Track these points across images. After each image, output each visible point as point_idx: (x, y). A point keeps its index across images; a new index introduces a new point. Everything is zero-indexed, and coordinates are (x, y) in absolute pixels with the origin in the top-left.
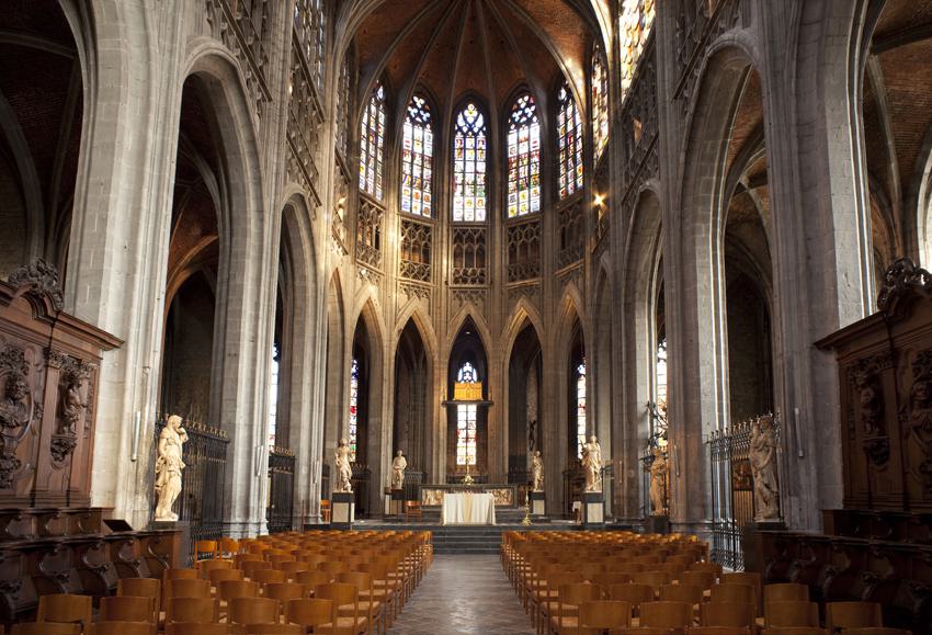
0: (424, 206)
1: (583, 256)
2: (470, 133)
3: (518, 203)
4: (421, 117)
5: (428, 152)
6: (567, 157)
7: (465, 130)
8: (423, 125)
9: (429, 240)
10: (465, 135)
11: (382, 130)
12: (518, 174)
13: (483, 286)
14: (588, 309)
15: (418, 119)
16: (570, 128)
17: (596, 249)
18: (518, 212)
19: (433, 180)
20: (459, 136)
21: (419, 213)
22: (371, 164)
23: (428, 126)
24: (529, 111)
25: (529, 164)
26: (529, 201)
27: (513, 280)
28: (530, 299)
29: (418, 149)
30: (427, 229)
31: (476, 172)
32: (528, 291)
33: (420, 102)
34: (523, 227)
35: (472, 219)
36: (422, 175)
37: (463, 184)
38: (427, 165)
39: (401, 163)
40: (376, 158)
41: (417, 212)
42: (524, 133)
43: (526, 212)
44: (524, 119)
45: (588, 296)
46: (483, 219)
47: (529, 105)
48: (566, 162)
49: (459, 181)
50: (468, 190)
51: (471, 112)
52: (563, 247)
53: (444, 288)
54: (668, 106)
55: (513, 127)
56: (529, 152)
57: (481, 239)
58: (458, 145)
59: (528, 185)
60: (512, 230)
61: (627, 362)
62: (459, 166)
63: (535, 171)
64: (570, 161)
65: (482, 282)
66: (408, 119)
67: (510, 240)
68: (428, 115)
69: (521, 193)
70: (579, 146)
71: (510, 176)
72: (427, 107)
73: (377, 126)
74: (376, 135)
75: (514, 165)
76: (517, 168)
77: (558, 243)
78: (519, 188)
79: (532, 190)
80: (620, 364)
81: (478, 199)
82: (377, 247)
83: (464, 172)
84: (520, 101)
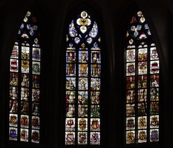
2: (83, 45)
7: (77, 41)
10: (77, 47)
12: (136, 97)
19: (42, 100)
20: (70, 48)
25: (149, 87)
29: (25, 70)
31: (90, 89)
37: (76, 103)
39: (8, 88)
49: (71, 99)
58: (69, 59)
63: (155, 98)
68: (36, 27)
71: (128, 98)
75: (132, 85)
76: (136, 90)
78: (137, 113)
83: (76, 90)
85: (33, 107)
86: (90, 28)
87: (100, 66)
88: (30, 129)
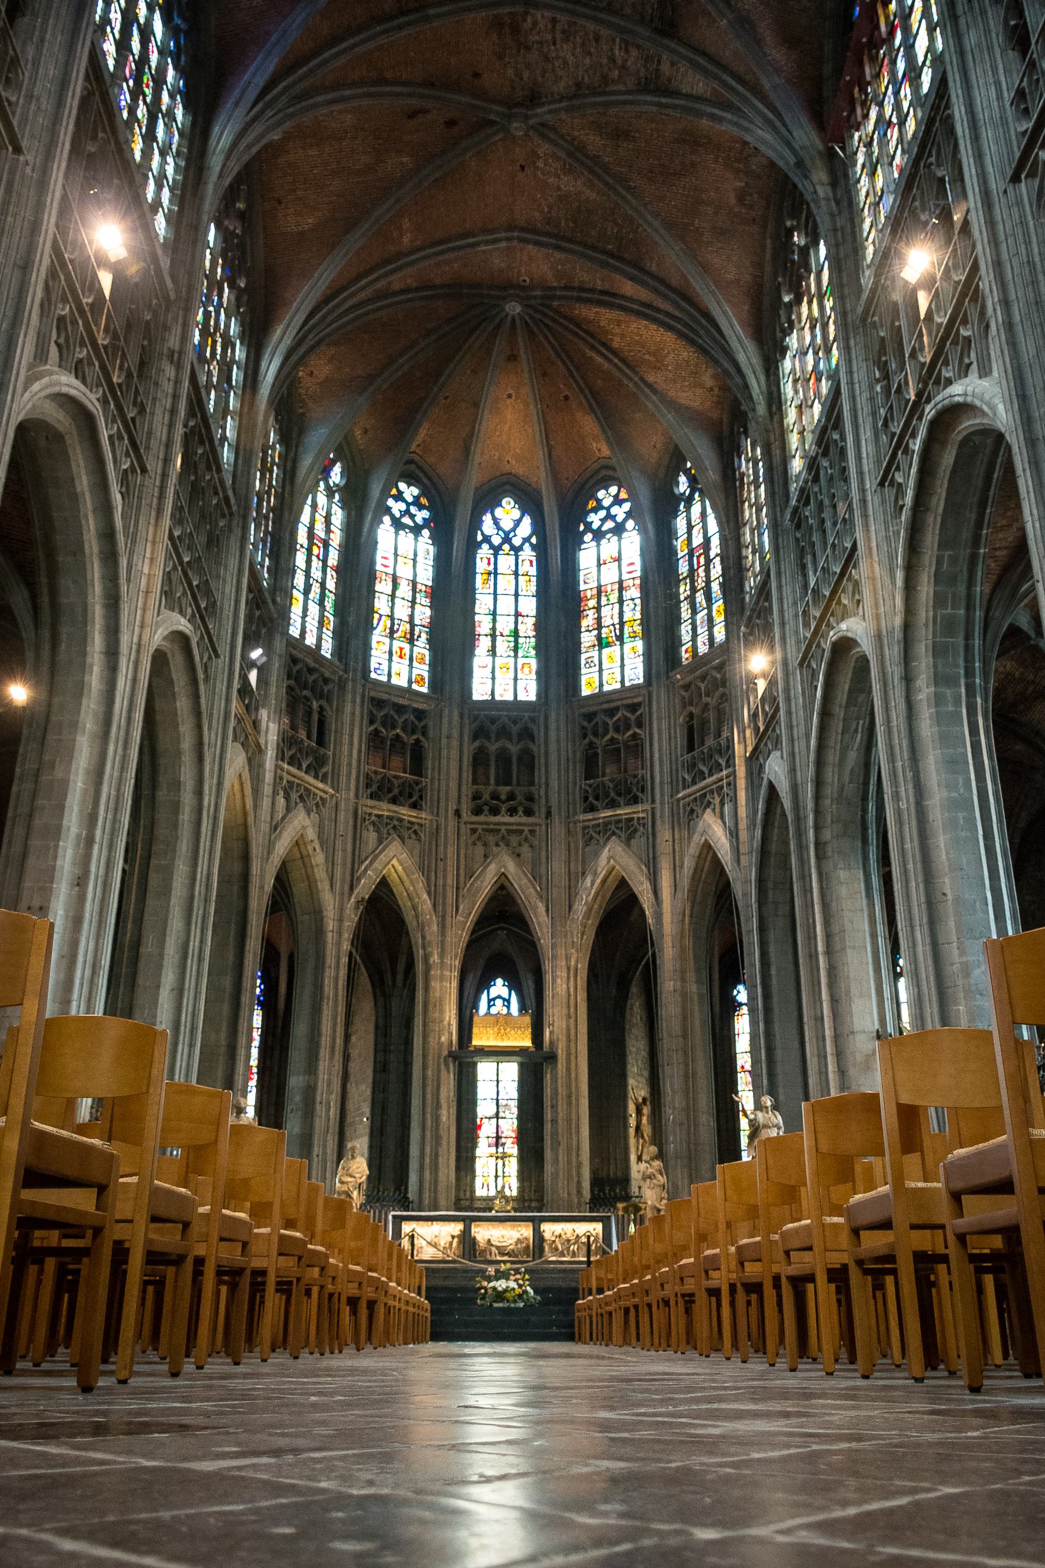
0: (415, 672)
1: (730, 762)
2: (506, 547)
3: (601, 670)
4: (412, 517)
5: (426, 576)
6: (694, 590)
7: (496, 540)
8: (416, 530)
9: (424, 733)
10: (496, 550)
11: (336, 538)
12: (599, 619)
13: (530, 820)
14: (744, 860)
15: (406, 520)
16: (697, 540)
17: (755, 749)
18: (601, 685)
19: (435, 628)
20: (484, 551)
21: (405, 685)
22: (316, 589)
23: (426, 533)
24: (620, 512)
25: (621, 601)
26: (622, 666)
27: (592, 809)
28: (628, 843)
29: (405, 572)
30: (420, 714)
32: (628, 830)
33: (410, 492)
34: (612, 712)
35: (509, 697)
36: (411, 617)
38: (423, 600)
39: (371, 593)
40: (323, 585)
41: (400, 681)
42: (609, 547)
43: (618, 686)
44: (610, 525)
45: (743, 835)
46: (532, 697)
47: (617, 501)
48: (692, 599)
50: (503, 646)
51: (508, 511)
52: (691, 748)
53: (452, 824)
54: (869, 498)
55: (588, 537)
56: (621, 583)
57: (527, 734)
58: (481, 566)
59: (620, 638)
60: (590, 717)
61: (829, 952)
62: (483, 603)
63: (633, 613)
64: (700, 597)
65: (529, 813)
66: (387, 519)
67: (585, 736)
68: (425, 514)
69: (606, 652)
70: (716, 570)
71: (584, 623)
72: (424, 501)
73: (328, 531)
74: (326, 544)
75: (592, 603)
76: (598, 608)
77: (681, 740)
78: (601, 643)
79: (627, 647)
80: (813, 956)
81: (520, 661)
82: (321, 741)
84: (601, 494)
85: (417, 633)
86: (517, 523)
87: (534, 579)
88: (411, 665)
